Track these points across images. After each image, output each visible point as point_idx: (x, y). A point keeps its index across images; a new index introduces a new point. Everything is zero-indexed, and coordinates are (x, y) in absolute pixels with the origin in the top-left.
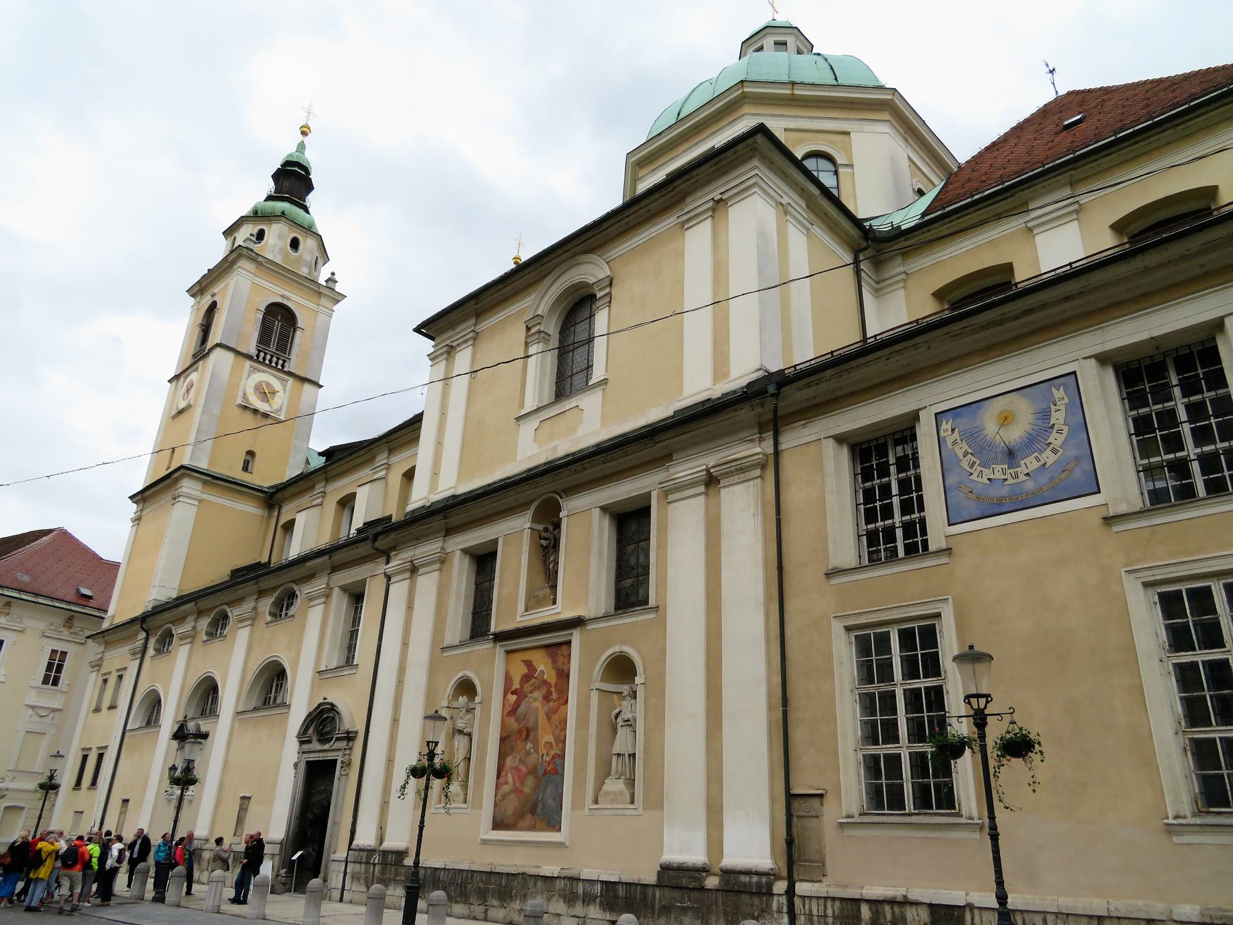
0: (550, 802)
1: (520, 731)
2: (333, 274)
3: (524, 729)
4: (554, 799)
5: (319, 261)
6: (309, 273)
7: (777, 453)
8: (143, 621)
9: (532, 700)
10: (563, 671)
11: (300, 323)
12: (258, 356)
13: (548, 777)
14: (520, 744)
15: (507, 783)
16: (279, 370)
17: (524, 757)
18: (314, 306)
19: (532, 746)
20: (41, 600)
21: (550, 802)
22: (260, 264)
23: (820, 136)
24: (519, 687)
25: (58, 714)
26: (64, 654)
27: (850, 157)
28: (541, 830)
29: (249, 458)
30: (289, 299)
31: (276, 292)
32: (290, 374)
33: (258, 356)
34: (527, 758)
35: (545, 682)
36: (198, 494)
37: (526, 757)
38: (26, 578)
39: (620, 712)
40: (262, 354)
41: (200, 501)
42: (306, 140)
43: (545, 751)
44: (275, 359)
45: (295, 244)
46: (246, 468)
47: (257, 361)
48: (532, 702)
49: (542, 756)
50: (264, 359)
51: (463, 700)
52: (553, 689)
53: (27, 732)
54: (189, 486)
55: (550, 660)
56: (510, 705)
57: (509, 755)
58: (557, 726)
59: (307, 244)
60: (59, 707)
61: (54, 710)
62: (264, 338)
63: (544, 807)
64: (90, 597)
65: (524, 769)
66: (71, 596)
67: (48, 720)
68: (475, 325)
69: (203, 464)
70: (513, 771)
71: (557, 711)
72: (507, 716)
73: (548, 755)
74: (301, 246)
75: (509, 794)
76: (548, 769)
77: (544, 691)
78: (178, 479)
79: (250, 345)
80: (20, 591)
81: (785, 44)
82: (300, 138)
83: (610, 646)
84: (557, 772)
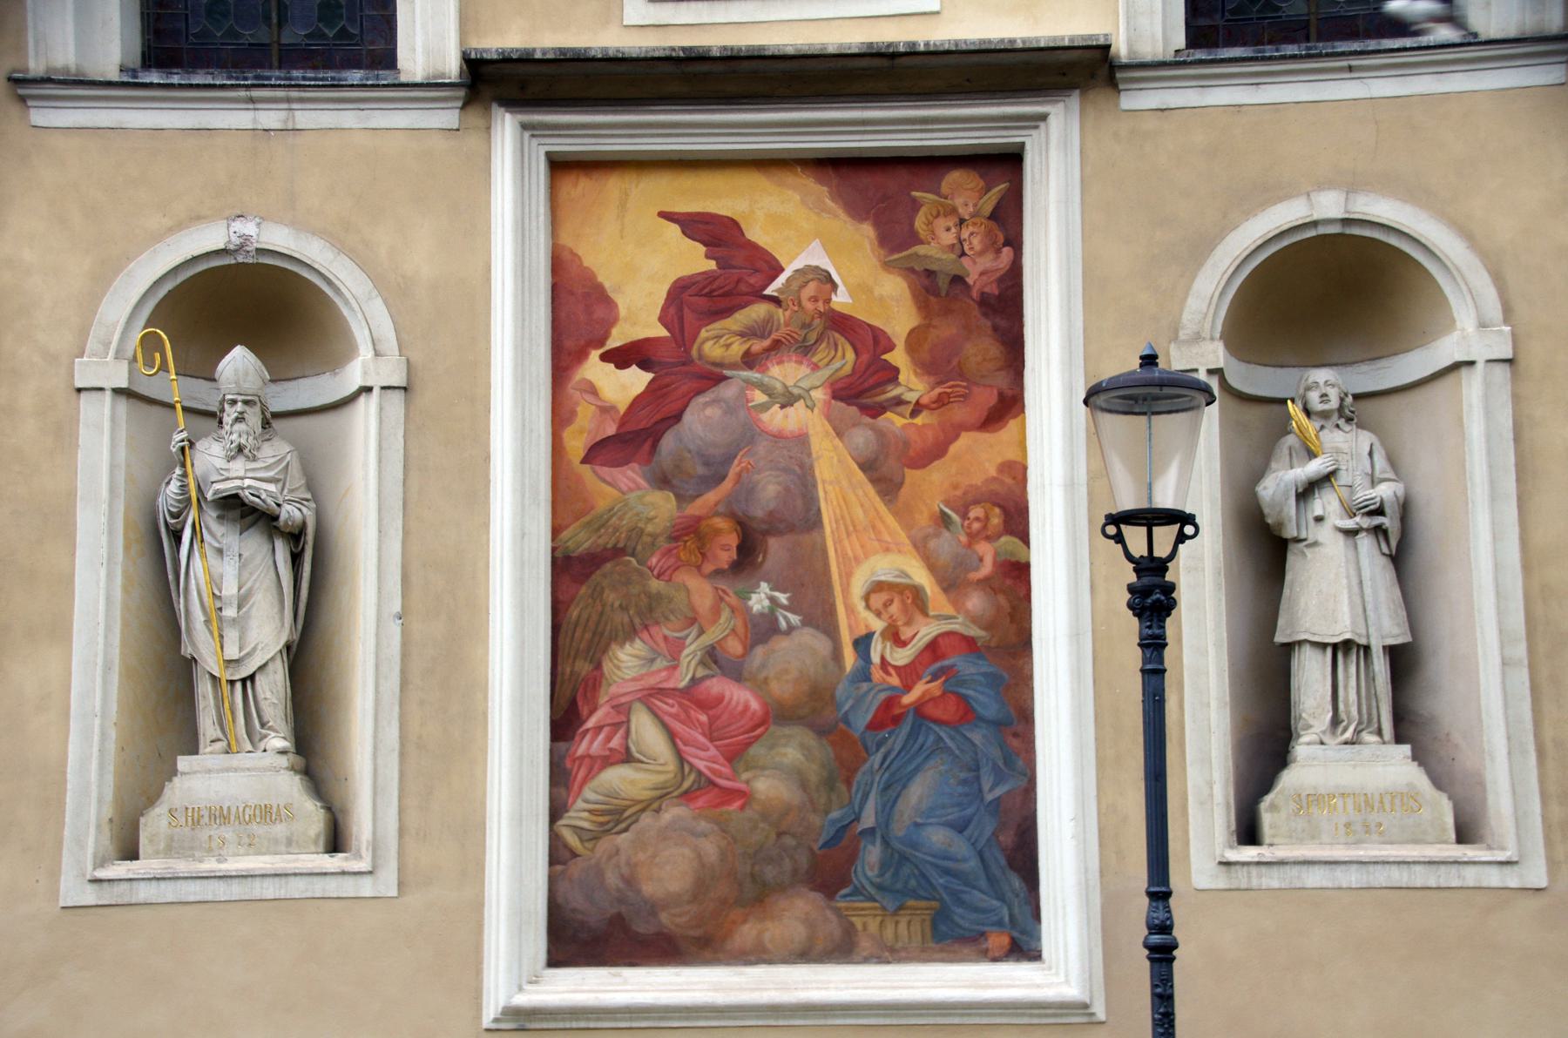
0: (938, 837)
1: (689, 533)
3: (720, 523)
4: (960, 827)
9: (759, 397)
10: (958, 280)
13: (914, 734)
14: (698, 590)
15: (627, 758)
17: (735, 647)
19: (783, 598)
21: (938, 837)
24: (661, 332)
28: (888, 954)
34: (759, 651)
35: (841, 324)
37: (749, 648)
39: (1326, 479)
43: (878, 625)
48: (764, 407)
49: (862, 644)
51: (238, 364)
52: (898, 357)
55: (868, 230)
56: (606, 410)
57: (631, 633)
58: (943, 513)
63: (896, 859)
65: (740, 696)
70: (669, 707)
71: (937, 451)
72: (585, 461)
73: (895, 638)
75: (654, 804)
76: (908, 699)
77: (845, 360)
83: (1273, 193)
84: (967, 714)
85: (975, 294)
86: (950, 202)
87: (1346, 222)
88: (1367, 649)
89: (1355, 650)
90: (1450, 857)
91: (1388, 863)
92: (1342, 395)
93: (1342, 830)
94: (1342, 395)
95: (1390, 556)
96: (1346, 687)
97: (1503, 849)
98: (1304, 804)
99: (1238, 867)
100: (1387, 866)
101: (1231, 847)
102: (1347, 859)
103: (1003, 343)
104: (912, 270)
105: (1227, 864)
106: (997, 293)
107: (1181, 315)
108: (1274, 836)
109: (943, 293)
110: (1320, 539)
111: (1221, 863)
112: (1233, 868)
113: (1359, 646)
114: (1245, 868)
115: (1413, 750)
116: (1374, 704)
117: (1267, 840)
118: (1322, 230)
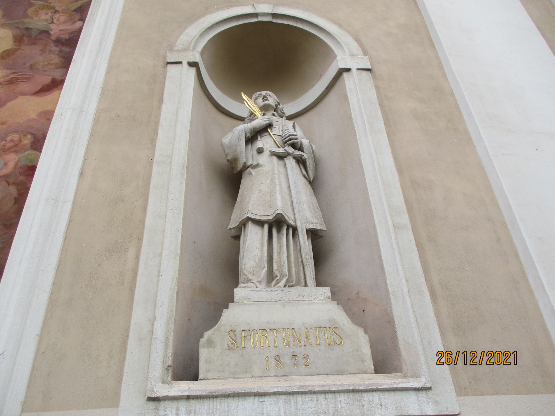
85: (53, 38)
86: (52, 5)
87: (274, 15)
88: (295, 230)
89: (285, 228)
90: (372, 384)
91: (315, 393)
92: (277, 103)
93: (273, 362)
94: (277, 103)
95: (310, 182)
96: (279, 254)
97: (416, 376)
98: (238, 340)
99: (167, 403)
100: (314, 397)
101: (164, 382)
102: (276, 390)
103: (64, 57)
104: (18, 28)
105: (156, 399)
106: (67, 38)
107: (176, 41)
108: (208, 371)
109: (33, 37)
110: (261, 162)
111: (150, 399)
112: (162, 403)
113: (289, 226)
114: (174, 404)
115: (332, 293)
116: (301, 269)
117: (200, 376)
118: (261, 19)
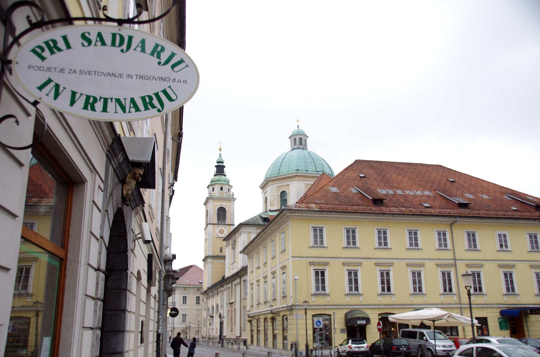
2: (233, 192)
5: (230, 189)
6: (227, 195)
7: (240, 282)
8: (205, 292)
11: (227, 211)
12: (218, 223)
16: (223, 225)
18: (229, 204)
20: (191, 286)
22: (213, 199)
23: (284, 187)
25: (201, 310)
26: (199, 297)
27: (289, 192)
29: (221, 249)
30: (222, 205)
31: (219, 204)
32: (227, 225)
33: (218, 223)
36: (211, 261)
38: (188, 281)
40: (219, 222)
41: (212, 263)
42: (221, 152)
44: (222, 222)
45: (222, 189)
46: (221, 252)
47: (218, 224)
50: (220, 223)
53: (196, 315)
54: (209, 260)
59: (225, 188)
60: (201, 309)
61: (200, 310)
62: (219, 218)
64: (201, 283)
66: (198, 284)
67: (199, 312)
68: (228, 242)
69: (211, 254)
74: (223, 189)
78: (207, 259)
79: (216, 221)
80: (186, 285)
81: (296, 138)
82: (219, 152)
